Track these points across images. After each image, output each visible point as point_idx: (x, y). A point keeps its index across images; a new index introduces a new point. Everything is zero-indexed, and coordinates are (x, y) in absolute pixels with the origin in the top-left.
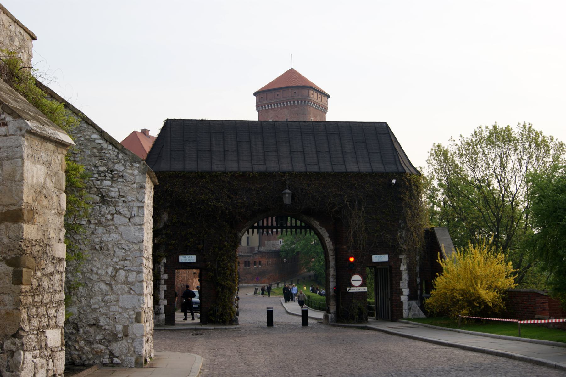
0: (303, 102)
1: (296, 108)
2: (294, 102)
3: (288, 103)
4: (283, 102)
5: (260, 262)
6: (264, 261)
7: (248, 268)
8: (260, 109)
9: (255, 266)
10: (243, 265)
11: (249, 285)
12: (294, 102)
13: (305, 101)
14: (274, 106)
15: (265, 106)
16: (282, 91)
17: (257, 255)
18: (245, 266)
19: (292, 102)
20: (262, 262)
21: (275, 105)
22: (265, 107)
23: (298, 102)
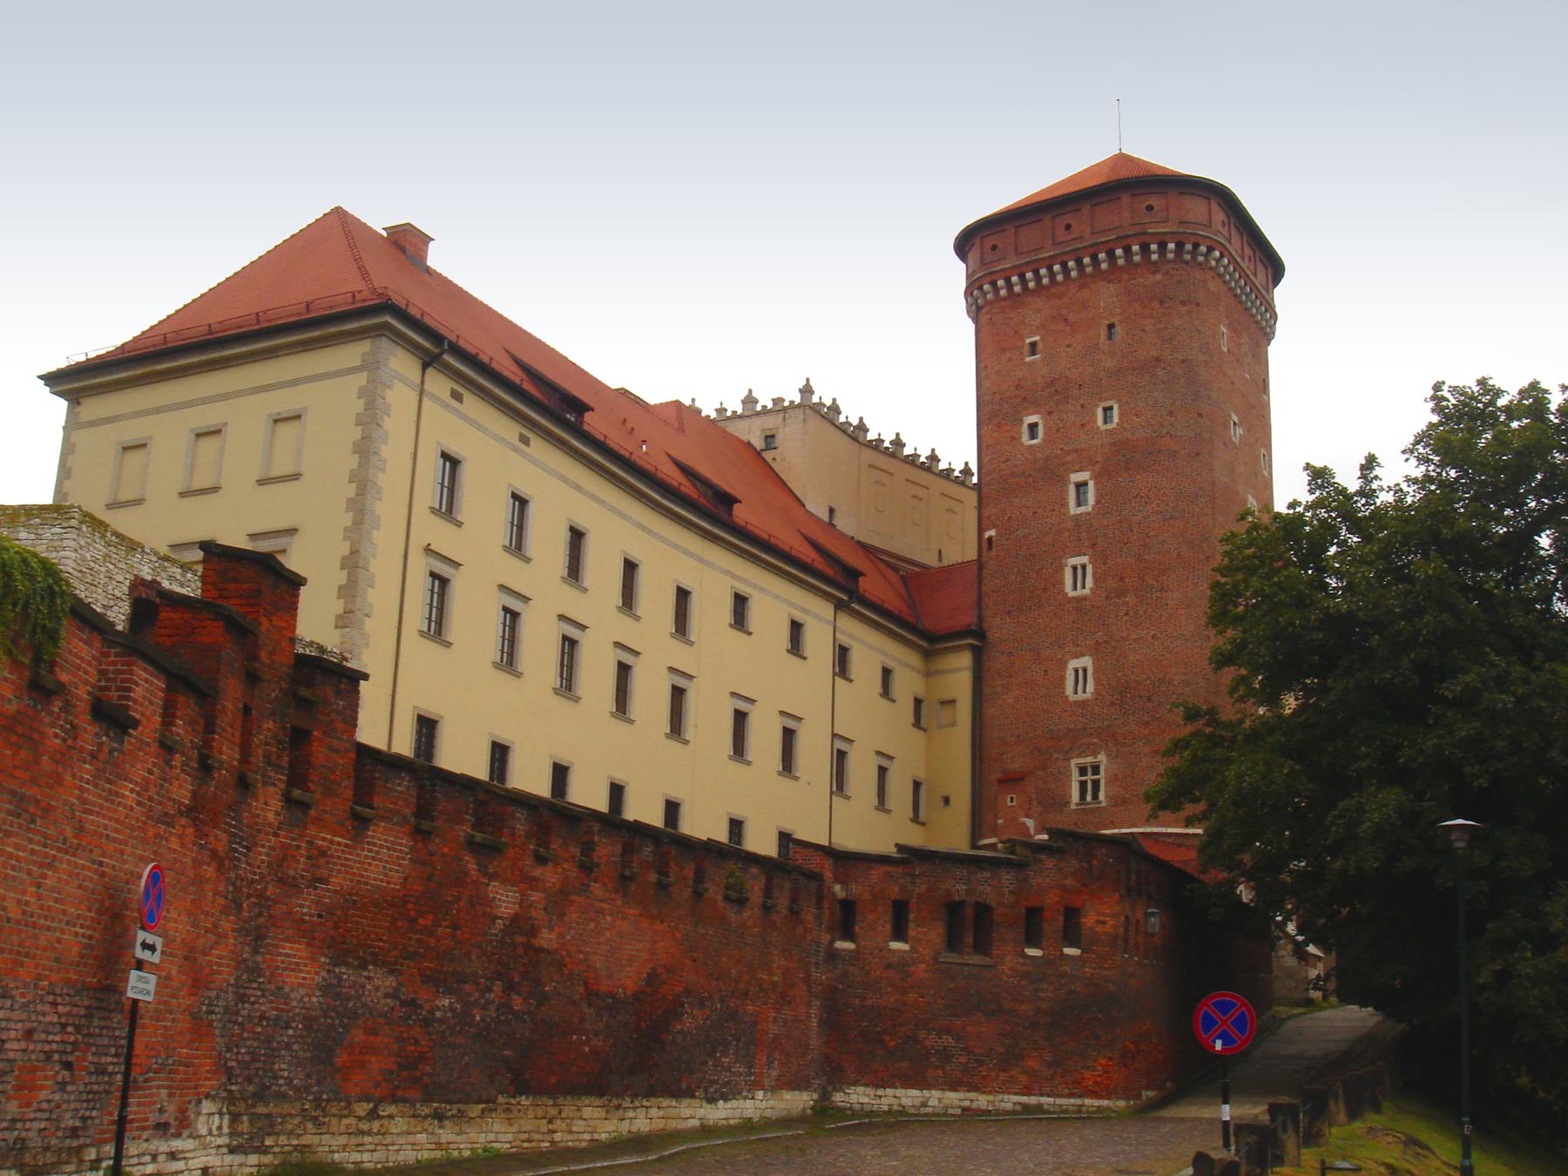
0: (1189, 247)
1: (1154, 273)
2: (1145, 248)
3: (1119, 252)
4: (1091, 250)
5: (1072, 914)
6: (1102, 916)
7: (975, 959)
8: (985, 294)
9: (1032, 952)
10: (936, 933)
11: (982, 1101)
12: (1145, 248)
13: (1196, 246)
14: (1052, 275)
15: (1008, 280)
16: (1086, 209)
17: (1049, 863)
18: (953, 941)
19: (1136, 248)
20: (1089, 920)
21: (1057, 268)
22: (1009, 285)
23: (1162, 246)
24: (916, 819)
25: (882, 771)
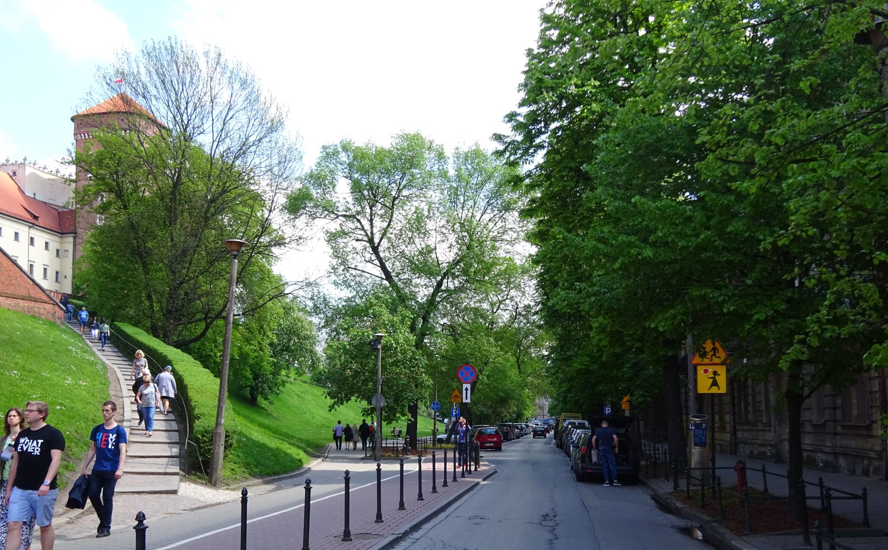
24: (57, 281)
25: (45, 269)
